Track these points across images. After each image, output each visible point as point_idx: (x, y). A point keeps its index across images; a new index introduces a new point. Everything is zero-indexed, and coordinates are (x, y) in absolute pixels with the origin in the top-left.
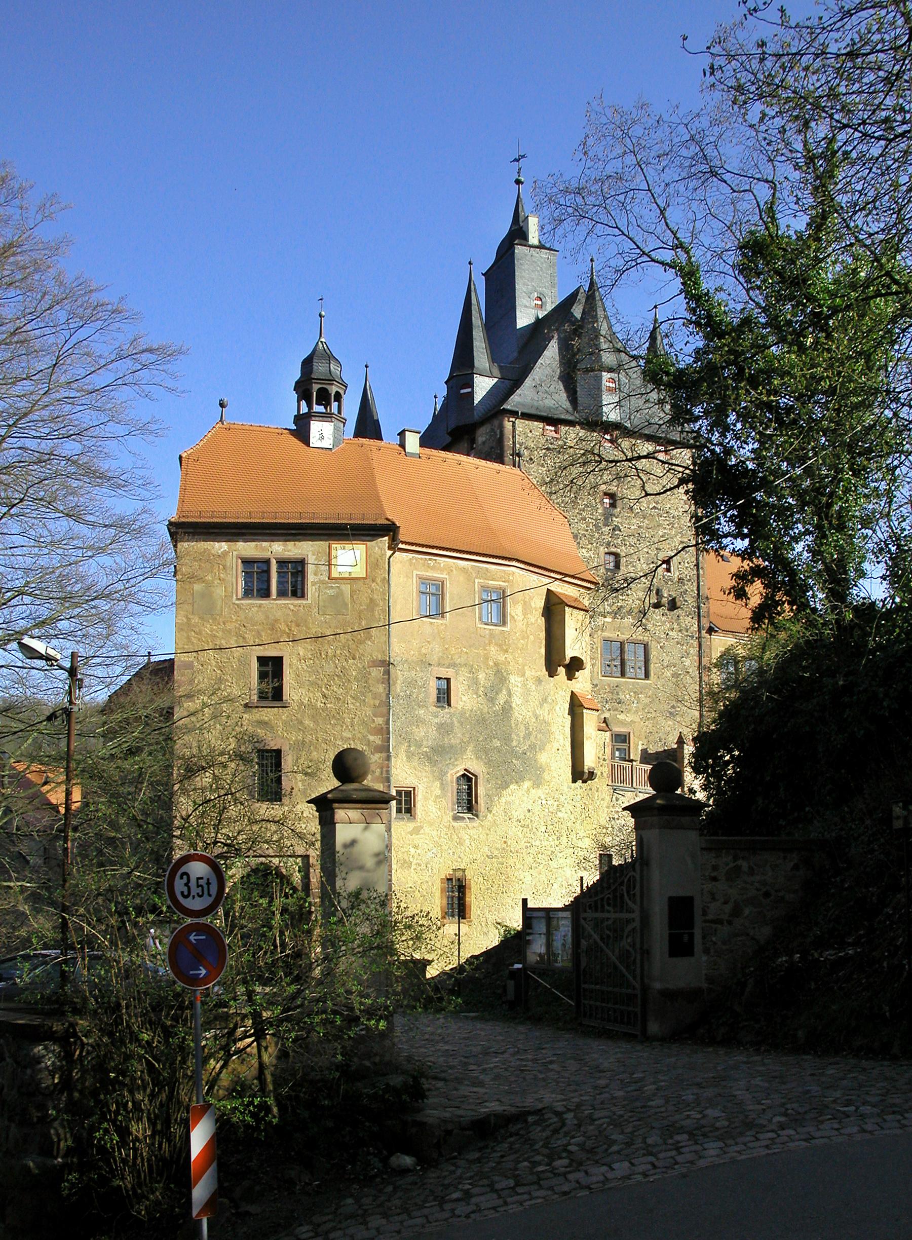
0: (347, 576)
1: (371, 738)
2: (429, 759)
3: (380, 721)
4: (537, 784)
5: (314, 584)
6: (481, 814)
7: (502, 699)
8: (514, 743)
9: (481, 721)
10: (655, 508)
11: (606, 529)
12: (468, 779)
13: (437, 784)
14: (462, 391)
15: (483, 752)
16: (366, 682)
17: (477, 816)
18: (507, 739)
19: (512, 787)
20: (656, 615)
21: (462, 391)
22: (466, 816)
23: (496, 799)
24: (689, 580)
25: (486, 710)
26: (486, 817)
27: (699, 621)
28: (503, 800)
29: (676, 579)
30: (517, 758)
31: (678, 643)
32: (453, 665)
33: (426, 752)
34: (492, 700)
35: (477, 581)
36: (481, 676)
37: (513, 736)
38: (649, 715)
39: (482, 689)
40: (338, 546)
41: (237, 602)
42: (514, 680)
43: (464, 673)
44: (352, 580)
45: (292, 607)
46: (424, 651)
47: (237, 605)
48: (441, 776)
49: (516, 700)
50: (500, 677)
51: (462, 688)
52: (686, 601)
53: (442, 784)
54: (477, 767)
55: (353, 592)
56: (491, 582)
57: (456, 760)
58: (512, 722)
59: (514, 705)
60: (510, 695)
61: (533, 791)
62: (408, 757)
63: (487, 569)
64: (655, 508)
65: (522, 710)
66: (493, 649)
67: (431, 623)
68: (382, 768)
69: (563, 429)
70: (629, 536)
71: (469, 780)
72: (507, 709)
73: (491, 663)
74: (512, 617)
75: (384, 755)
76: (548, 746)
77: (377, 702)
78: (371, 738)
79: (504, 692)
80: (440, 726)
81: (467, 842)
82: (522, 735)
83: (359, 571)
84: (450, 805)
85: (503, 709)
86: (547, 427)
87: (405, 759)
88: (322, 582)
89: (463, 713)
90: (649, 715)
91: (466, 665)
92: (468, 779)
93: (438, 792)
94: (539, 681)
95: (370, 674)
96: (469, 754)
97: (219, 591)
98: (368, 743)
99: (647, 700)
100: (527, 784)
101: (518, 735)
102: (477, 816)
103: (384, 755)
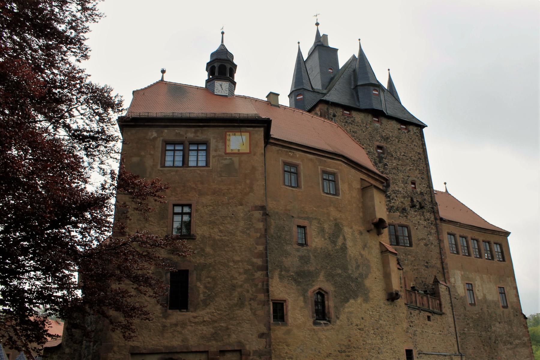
0: (237, 152)
1: (255, 260)
2: (295, 280)
3: (261, 248)
4: (366, 300)
5: (214, 157)
6: (332, 320)
7: (340, 242)
8: (350, 272)
9: (328, 256)
10: (404, 155)
11: (380, 165)
12: (321, 293)
13: (301, 298)
14: (298, 98)
15: (330, 277)
16: (250, 221)
17: (329, 321)
18: (345, 268)
19: (352, 301)
20: (412, 212)
21: (298, 98)
22: (322, 322)
23: (342, 309)
24: (426, 194)
25: (330, 249)
26: (335, 322)
27: (435, 216)
28: (346, 310)
29: (419, 193)
30: (352, 282)
31: (425, 227)
32: (307, 218)
33: (292, 275)
34: (334, 242)
35: (319, 167)
36: (326, 226)
37: (350, 267)
38: (415, 268)
39: (327, 235)
40: (231, 133)
41: (161, 169)
42: (346, 229)
43: (315, 223)
44: (239, 154)
45: (198, 172)
46: (288, 208)
47: (161, 171)
48: (304, 293)
49: (349, 243)
50: (338, 228)
51: (314, 233)
52: (426, 204)
53: (304, 298)
54: (328, 287)
55: (240, 162)
56: (328, 169)
57: (313, 281)
58: (348, 257)
59: (348, 247)
60: (345, 239)
61: (364, 305)
62: (280, 278)
63: (325, 161)
64: (404, 155)
65: (353, 250)
66: (332, 209)
67: (292, 190)
68: (263, 282)
69: (354, 114)
70: (392, 169)
71: (323, 296)
72: (344, 248)
73: (332, 219)
74: (342, 191)
75: (265, 272)
76: (370, 276)
77: (258, 235)
78: (255, 260)
79: (341, 237)
80: (301, 258)
81: (324, 340)
82: (354, 266)
83: (245, 149)
84: (311, 313)
85: (341, 248)
86: (345, 112)
87: (278, 280)
88: (220, 156)
89: (315, 249)
90: (415, 268)
91: (316, 219)
92: (321, 293)
93: (302, 304)
94: (361, 233)
95: (253, 215)
96: (321, 277)
97: (149, 163)
98: (253, 264)
99: (413, 259)
100: (359, 300)
101: (352, 267)
102: (329, 321)
103: (265, 272)
